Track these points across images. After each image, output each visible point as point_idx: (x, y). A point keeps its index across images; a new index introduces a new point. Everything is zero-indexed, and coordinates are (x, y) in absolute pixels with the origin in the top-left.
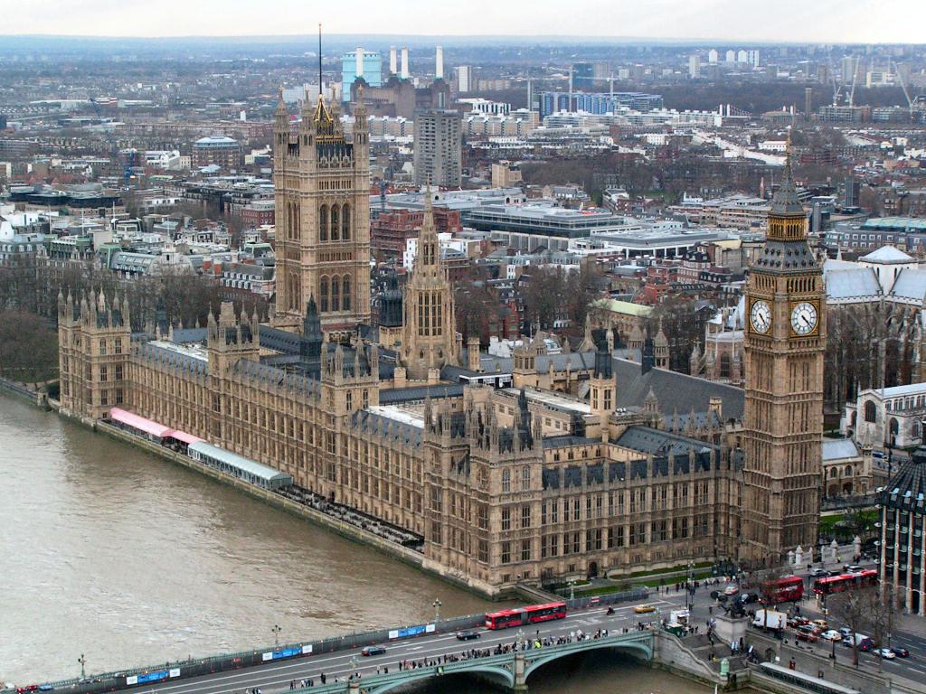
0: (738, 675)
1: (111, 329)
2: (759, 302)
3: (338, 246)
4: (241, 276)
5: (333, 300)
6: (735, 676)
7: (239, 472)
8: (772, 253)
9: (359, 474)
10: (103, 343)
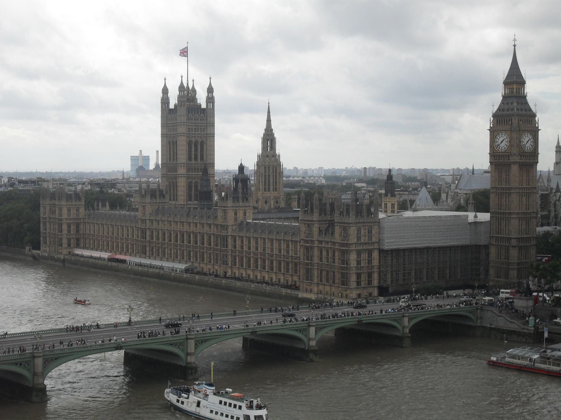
0: (539, 327)
1: (73, 203)
2: (500, 134)
3: (197, 164)
4: (129, 199)
5: (195, 195)
6: (538, 327)
7: (161, 268)
8: (507, 104)
9: (244, 257)
10: (69, 210)
